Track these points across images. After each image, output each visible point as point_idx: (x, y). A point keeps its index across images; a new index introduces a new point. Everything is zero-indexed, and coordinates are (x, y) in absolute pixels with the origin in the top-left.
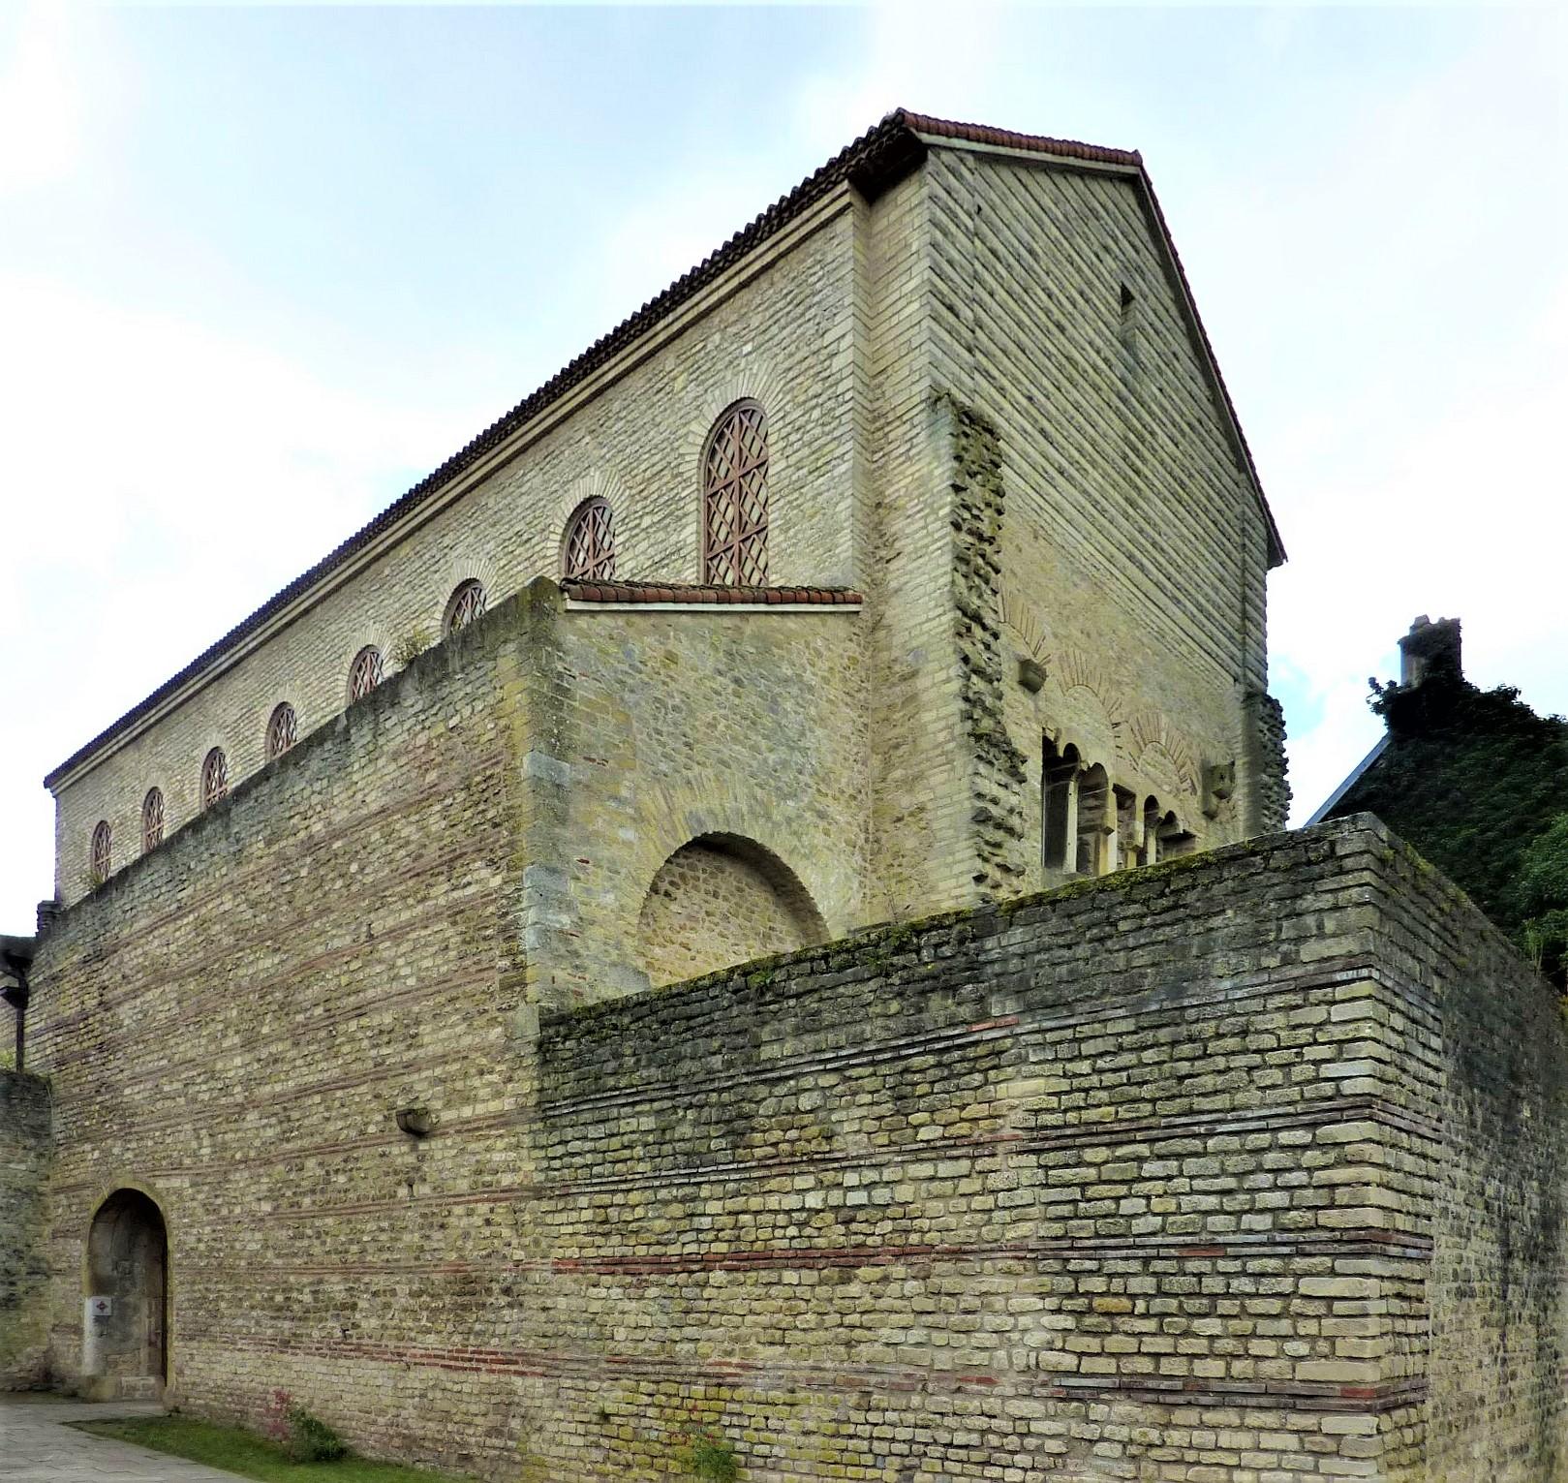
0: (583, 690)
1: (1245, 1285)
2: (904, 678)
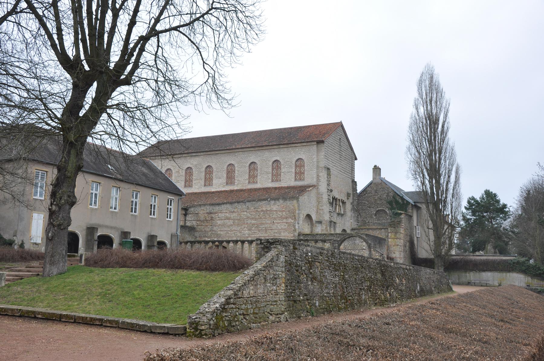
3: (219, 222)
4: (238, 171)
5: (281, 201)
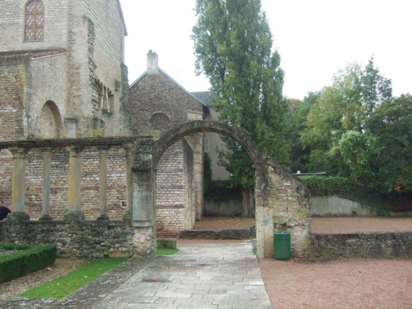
0: (33, 74)
1: (167, 192)
2: (76, 69)
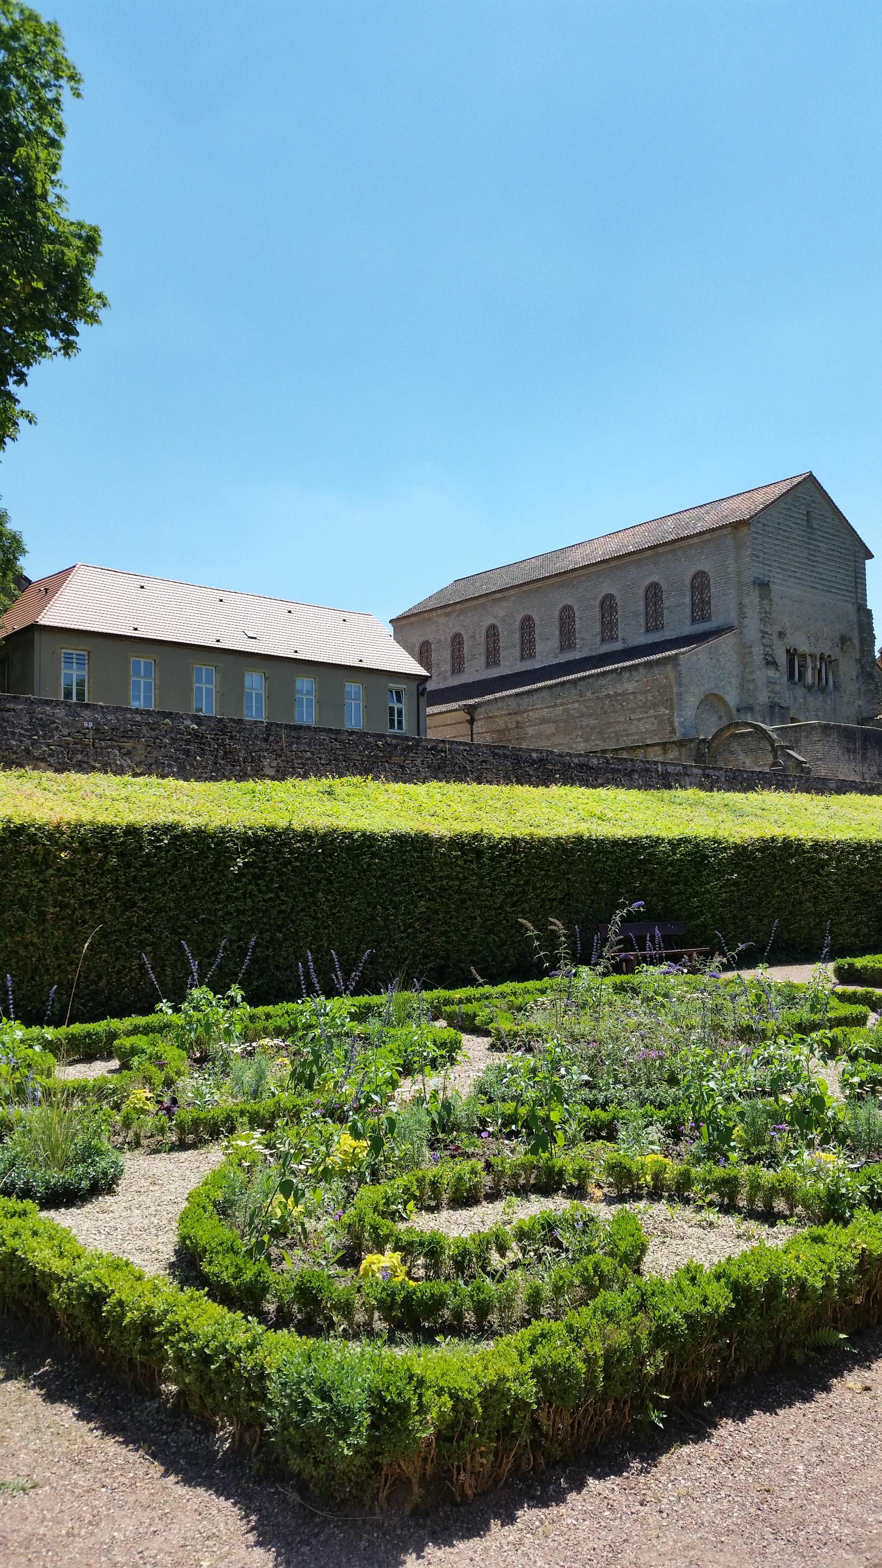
0: (684, 672)
3: (531, 731)
4: (580, 619)
5: (642, 670)
